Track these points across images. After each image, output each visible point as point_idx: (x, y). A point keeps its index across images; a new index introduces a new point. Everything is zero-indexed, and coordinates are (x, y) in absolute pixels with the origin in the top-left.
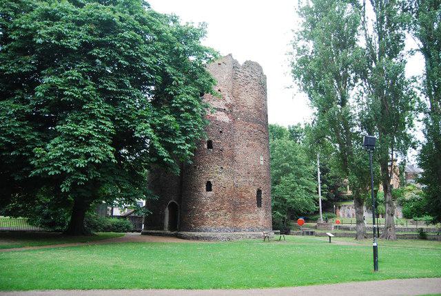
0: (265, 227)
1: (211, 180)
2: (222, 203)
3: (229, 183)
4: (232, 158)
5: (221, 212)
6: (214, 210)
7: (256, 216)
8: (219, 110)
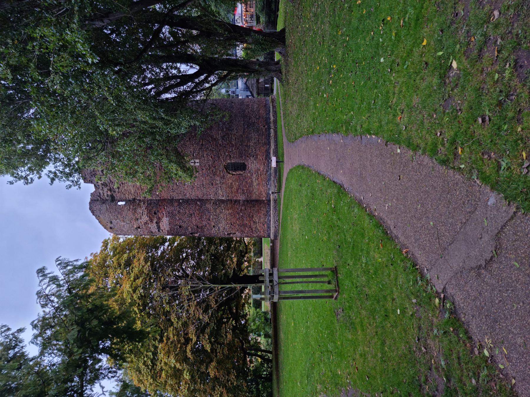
0: (266, 159)
1: (226, 233)
2: (245, 226)
3: (227, 218)
4: (200, 203)
5: (254, 226)
6: (252, 232)
7: (255, 176)
8: (159, 228)
